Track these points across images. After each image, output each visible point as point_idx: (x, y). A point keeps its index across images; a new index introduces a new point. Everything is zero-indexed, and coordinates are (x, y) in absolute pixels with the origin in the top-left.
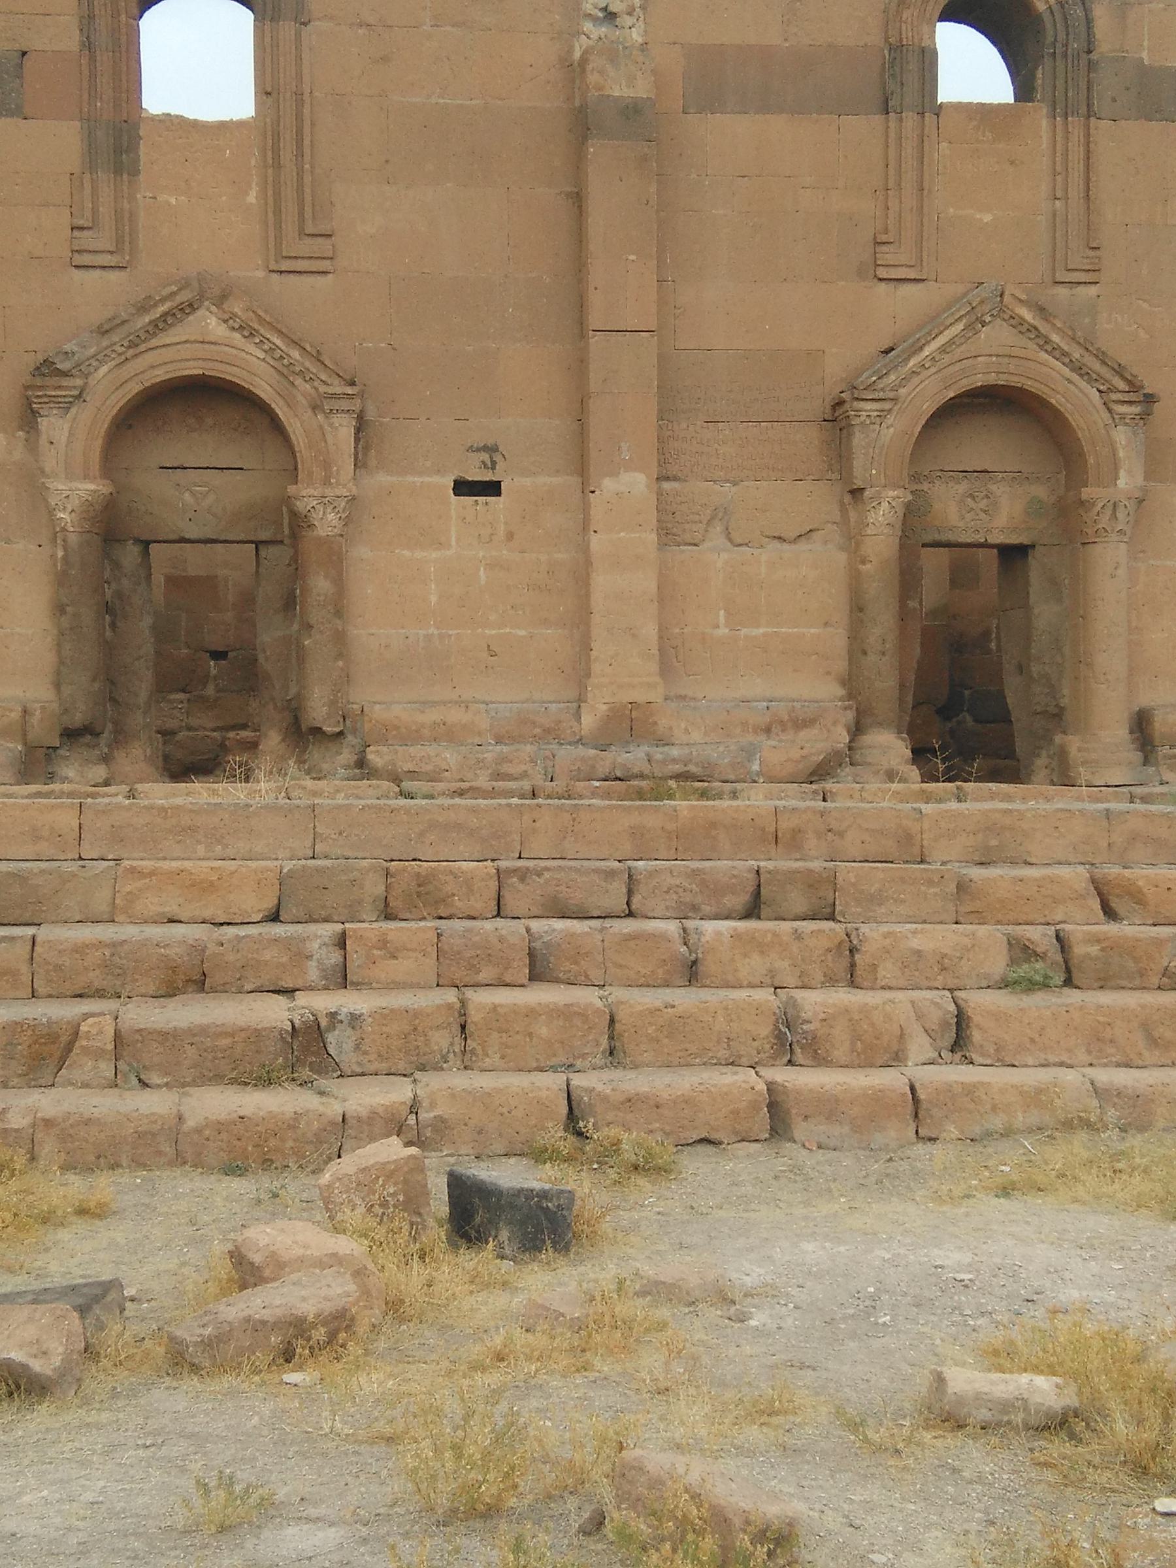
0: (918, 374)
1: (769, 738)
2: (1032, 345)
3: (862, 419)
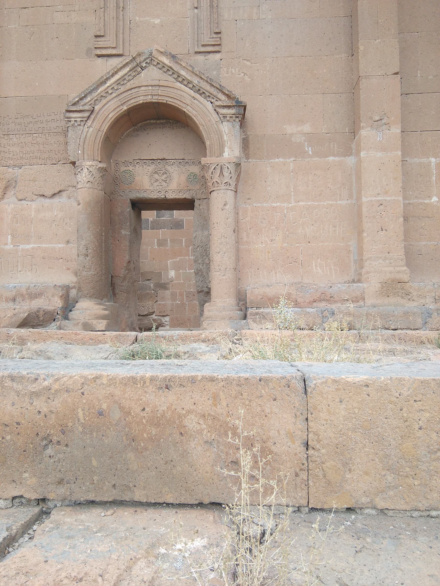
0: (105, 97)
1: (14, 304)
2: (171, 79)
3: (72, 123)
